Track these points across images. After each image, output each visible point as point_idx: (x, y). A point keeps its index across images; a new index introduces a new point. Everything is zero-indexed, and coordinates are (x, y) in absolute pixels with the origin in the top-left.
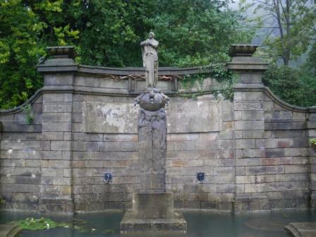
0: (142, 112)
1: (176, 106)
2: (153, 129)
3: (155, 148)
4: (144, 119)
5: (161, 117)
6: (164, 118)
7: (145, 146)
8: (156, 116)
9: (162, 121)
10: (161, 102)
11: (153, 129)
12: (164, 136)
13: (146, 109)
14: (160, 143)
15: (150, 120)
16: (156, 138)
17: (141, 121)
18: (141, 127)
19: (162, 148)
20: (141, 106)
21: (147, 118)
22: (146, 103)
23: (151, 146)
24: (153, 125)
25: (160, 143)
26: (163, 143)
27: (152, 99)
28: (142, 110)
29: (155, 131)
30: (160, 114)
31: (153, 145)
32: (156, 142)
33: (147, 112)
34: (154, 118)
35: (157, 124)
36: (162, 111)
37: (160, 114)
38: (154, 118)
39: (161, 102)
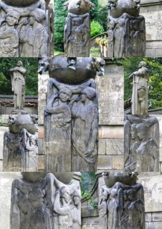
0: (54, 85)
1: (111, 80)
2: (74, 118)
3: (77, 154)
4: (58, 98)
5: (89, 94)
6: (94, 98)
7: (57, 149)
8: (80, 94)
9: (90, 104)
10: (88, 67)
11: (74, 118)
12: (95, 131)
13: (62, 81)
14: (87, 145)
15: (68, 101)
16: (79, 135)
17: (50, 101)
18: (50, 114)
19: (88, 155)
20: (52, 74)
21: (63, 96)
22: (62, 69)
23: (68, 149)
24: (74, 111)
25: (87, 145)
26: (92, 144)
27: (73, 62)
28: (54, 80)
29: (78, 121)
30: (88, 90)
31: (72, 147)
32: (79, 142)
33: (62, 86)
34: (75, 97)
35: (81, 109)
36: (90, 85)
37: (88, 90)
38: (75, 97)
39: (88, 67)
